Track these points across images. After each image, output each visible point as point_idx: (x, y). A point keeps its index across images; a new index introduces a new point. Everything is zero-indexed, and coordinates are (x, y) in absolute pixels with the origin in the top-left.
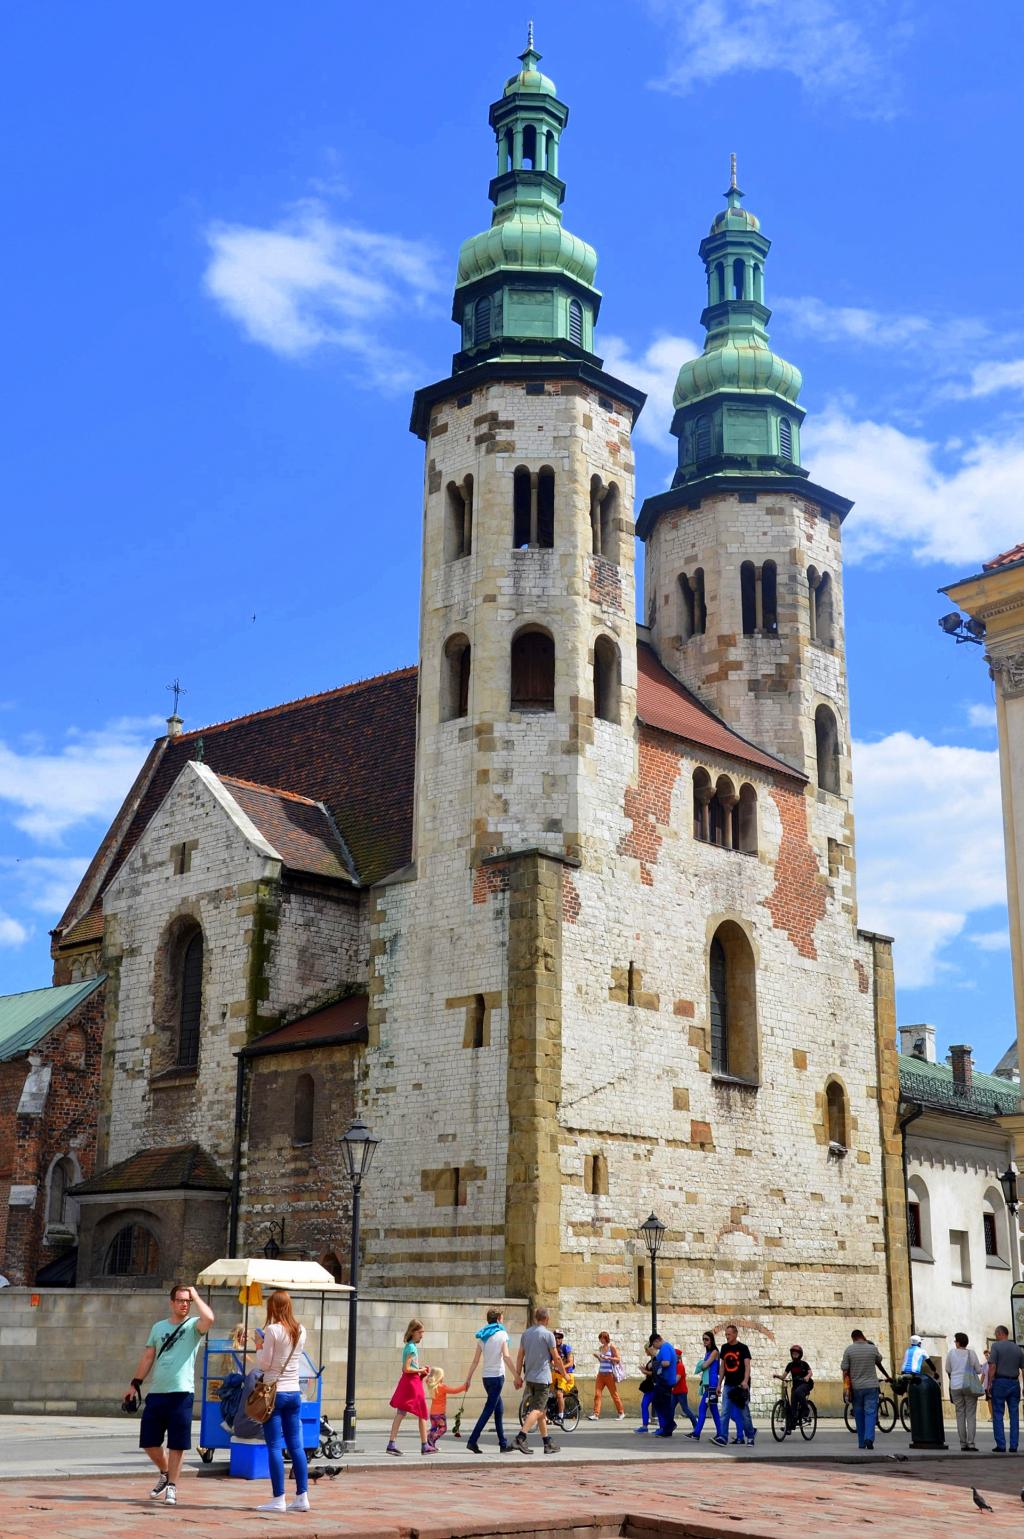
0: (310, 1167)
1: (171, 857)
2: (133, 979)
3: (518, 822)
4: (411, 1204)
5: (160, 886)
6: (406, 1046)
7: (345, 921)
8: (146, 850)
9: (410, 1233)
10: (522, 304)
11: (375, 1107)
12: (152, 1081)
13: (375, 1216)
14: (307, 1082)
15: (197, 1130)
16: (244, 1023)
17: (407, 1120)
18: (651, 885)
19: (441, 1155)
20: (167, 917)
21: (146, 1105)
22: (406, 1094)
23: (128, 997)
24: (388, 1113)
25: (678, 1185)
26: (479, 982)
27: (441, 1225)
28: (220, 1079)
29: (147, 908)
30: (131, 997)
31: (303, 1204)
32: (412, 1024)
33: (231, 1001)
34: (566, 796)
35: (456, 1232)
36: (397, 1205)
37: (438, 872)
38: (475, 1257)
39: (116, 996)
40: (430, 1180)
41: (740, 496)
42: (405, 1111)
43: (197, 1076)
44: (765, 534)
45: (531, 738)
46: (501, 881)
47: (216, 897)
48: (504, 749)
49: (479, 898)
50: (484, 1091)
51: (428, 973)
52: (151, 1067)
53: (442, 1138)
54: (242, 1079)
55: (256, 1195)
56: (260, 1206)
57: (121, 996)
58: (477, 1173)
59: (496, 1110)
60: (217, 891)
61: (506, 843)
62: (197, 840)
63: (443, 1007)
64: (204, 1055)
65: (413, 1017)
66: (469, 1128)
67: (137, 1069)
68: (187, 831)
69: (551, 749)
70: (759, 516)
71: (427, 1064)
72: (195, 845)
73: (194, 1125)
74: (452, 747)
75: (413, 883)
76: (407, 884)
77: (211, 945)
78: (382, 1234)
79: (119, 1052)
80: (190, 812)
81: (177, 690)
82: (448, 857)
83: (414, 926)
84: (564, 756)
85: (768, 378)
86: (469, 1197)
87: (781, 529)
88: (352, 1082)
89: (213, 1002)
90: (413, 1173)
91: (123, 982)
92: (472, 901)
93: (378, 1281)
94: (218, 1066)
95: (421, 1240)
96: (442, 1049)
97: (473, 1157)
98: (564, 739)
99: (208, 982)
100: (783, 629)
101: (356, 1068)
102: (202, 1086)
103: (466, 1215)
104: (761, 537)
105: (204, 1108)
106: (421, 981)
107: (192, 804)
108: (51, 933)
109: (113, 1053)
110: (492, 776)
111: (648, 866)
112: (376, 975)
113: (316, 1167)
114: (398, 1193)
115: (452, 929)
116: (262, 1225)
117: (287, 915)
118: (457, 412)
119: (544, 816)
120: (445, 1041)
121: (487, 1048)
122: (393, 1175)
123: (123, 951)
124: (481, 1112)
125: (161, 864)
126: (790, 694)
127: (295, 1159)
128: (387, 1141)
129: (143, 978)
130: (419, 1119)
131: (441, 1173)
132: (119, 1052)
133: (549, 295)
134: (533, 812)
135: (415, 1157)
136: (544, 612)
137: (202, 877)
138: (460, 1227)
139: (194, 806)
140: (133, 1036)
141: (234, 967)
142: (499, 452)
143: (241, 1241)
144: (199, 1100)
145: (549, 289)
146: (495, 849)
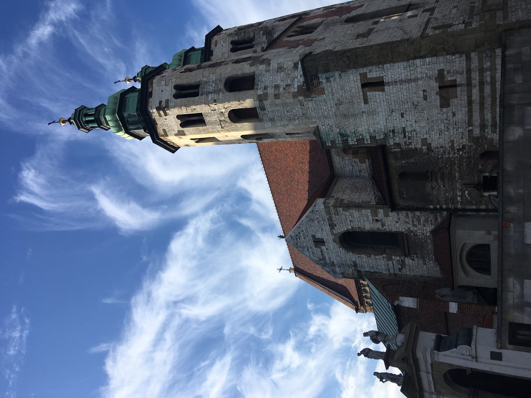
0: (440, 172)
1: (319, 247)
2: (366, 265)
3: (294, 80)
4: (456, 113)
5: (330, 252)
6: (385, 124)
7: (344, 180)
8: (317, 259)
9: (470, 112)
10: (128, 107)
11: (412, 138)
12: (406, 256)
13: (462, 133)
14: (403, 175)
15: (425, 232)
16: (379, 210)
17: (417, 120)
18: (325, 38)
19: (433, 97)
20: (341, 249)
21: (416, 259)
22: (406, 122)
23: (373, 267)
24: (415, 131)
25: (449, 10)
26: (356, 86)
27: (466, 93)
28: (403, 221)
29: (338, 259)
30: (372, 266)
31: (457, 174)
32: (376, 122)
33: (371, 217)
34: (285, 62)
35: (469, 84)
36: (457, 120)
37: (314, 115)
38: (482, 71)
39: (372, 272)
40: (445, 103)
41: (211, 56)
42: (413, 121)
43: (403, 233)
44: (222, 46)
45: (263, 79)
46: (315, 80)
47: (332, 226)
48: (267, 89)
49: (322, 92)
50: (403, 76)
51: (354, 115)
52: (400, 256)
53: (425, 98)
54: (402, 209)
55: (453, 200)
56: (458, 198)
57: (372, 270)
58: (441, 74)
59: (412, 68)
60: (330, 225)
61: (302, 84)
62: (312, 235)
63: (368, 105)
64: (394, 230)
65: (373, 121)
66: (420, 82)
67: (401, 263)
68: (309, 241)
69: (268, 71)
70: (217, 49)
71: (393, 111)
72: (314, 236)
73: (423, 234)
74: (267, 113)
75: (320, 128)
76: (320, 131)
77: (350, 228)
78: (471, 128)
79: (394, 272)
80: (302, 239)
81: (281, 269)
82: (308, 111)
83: (336, 126)
84: (271, 65)
85: (180, 56)
86: (453, 78)
87: (221, 41)
88: (402, 152)
89: (372, 226)
90: (442, 113)
91: (367, 269)
92: (324, 95)
93: (493, 128)
94: (397, 222)
95: (473, 105)
96: (385, 103)
97: (434, 79)
98: (264, 67)
99: (364, 229)
100: (252, 35)
101: (396, 150)
102: (406, 230)
103: (460, 79)
104: (224, 47)
105: (416, 229)
106: (358, 119)
107: (299, 238)
108: (357, 312)
109: (395, 274)
110: (276, 93)
111: (318, 40)
112: (356, 143)
113: (440, 168)
114: (451, 121)
115: (336, 104)
116: (467, 196)
117: (339, 196)
118: (158, 126)
119: (292, 70)
120: (382, 102)
121: (384, 78)
122: (443, 124)
123: (355, 270)
124: (413, 77)
125: (322, 252)
126: (272, 29)
127: (436, 180)
128: (427, 130)
129: (365, 261)
130: (417, 113)
131: (442, 98)
132: (394, 272)
133: (127, 98)
134: (290, 74)
135: (434, 112)
136: (221, 81)
137: (325, 233)
138: (467, 82)
139: (300, 237)
140: (388, 265)
141: (358, 216)
142: (168, 105)
143: (474, 207)
144: (412, 231)
145: (125, 99)
146: (304, 88)
